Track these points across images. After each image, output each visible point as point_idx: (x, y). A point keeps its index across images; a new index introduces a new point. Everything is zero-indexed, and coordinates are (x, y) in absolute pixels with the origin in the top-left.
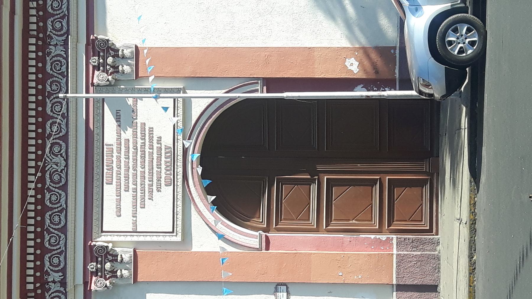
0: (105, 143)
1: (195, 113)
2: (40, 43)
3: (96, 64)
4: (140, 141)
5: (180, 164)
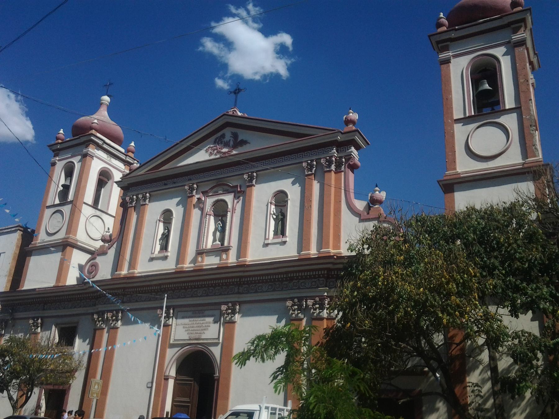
4: (204, 325)
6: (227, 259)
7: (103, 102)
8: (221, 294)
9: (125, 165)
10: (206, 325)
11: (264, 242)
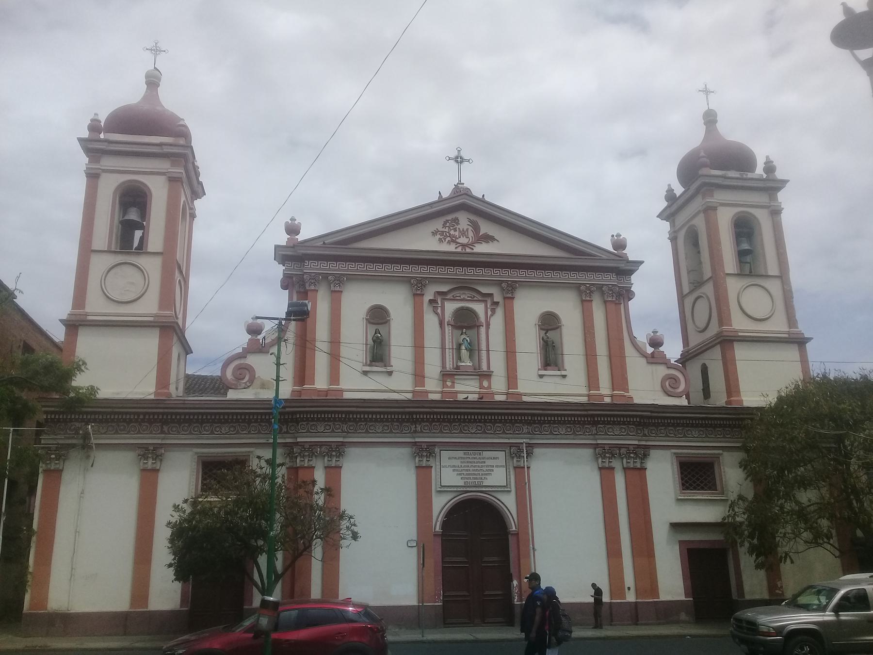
1: (499, 496)
2: (528, 421)
4: (485, 469)
5: (474, 489)
6: (489, 387)
8: (504, 433)
9: (191, 197)
10: (487, 468)
11: (538, 373)
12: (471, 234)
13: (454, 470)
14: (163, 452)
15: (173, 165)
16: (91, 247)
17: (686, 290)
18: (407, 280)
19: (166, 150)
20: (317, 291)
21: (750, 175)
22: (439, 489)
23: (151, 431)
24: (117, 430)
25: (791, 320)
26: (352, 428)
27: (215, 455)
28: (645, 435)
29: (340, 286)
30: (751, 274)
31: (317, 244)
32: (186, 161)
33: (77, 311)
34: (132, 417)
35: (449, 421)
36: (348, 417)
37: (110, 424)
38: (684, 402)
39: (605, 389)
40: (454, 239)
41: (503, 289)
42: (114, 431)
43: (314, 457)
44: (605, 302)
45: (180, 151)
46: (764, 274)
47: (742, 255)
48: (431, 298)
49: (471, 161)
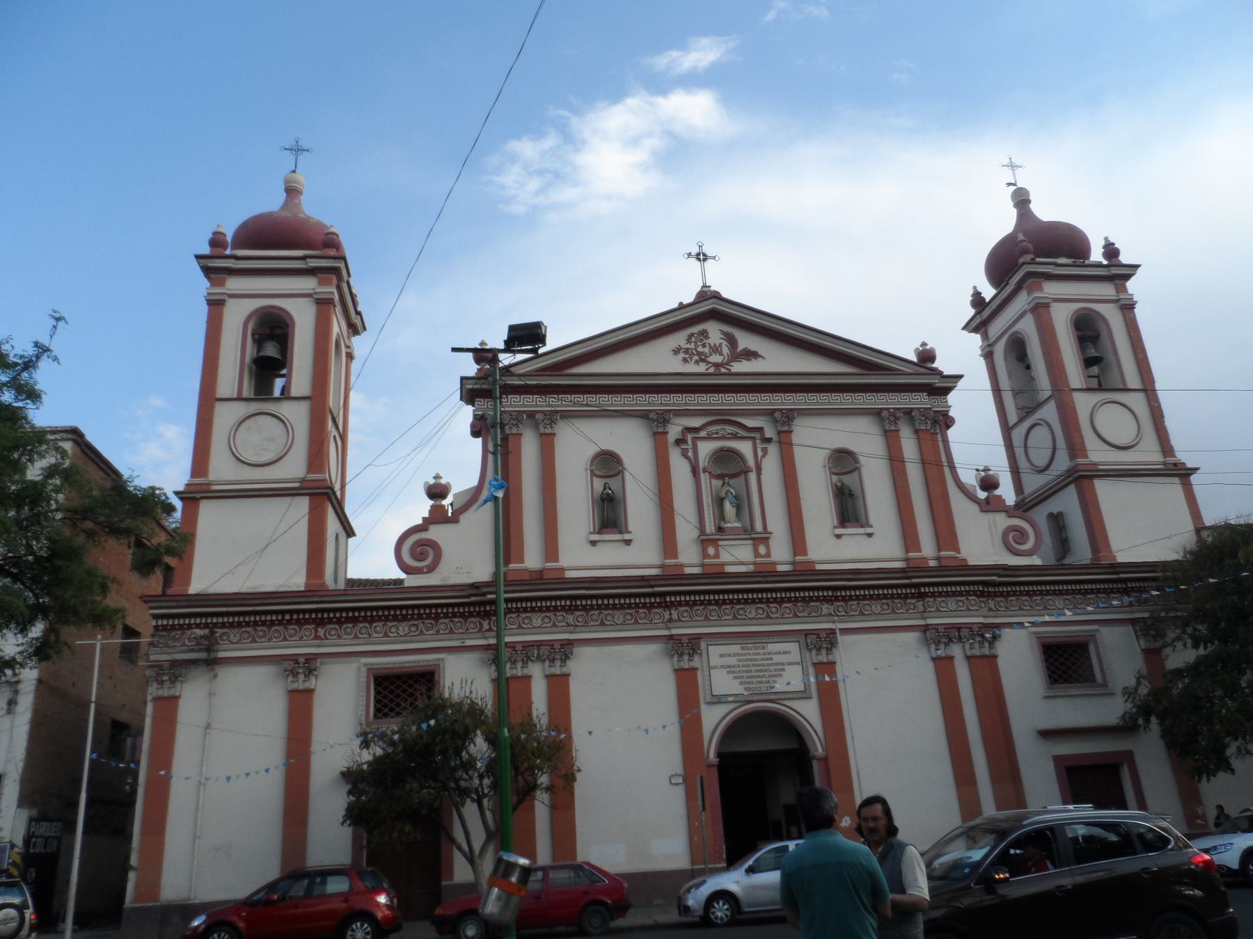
0: (769, 645)
1: (796, 704)
2: (829, 598)
3: (821, 636)
4: (772, 668)
5: (760, 697)
6: (768, 555)
7: (296, 185)
8: (796, 616)
9: (348, 332)
10: (776, 667)
12: (726, 350)
13: (729, 672)
14: (318, 665)
15: (321, 283)
16: (215, 395)
17: (1013, 418)
18: (643, 415)
19: (313, 263)
20: (521, 434)
21: (1087, 262)
22: (708, 699)
23: (302, 637)
24: (254, 638)
25: (1166, 447)
26: (580, 619)
27: (391, 666)
28: (990, 609)
29: (552, 427)
30: (1101, 388)
31: (518, 372)
32: (340, 278)
33: (197, 480)
34: (274, 618)
35: (717, 603)
36: (574, 604)
37: (244, 629)
38: (1036, 561)
39: (928, 548)
40: (703, 357)
41: (775, 421)
42: (251, 639)
43: (530, 664)
44: (917, 432)
45: (329, 265)
46: (1121, 387)
47: (1089, 362)
48: (678, 438)
49: (717, 258)
